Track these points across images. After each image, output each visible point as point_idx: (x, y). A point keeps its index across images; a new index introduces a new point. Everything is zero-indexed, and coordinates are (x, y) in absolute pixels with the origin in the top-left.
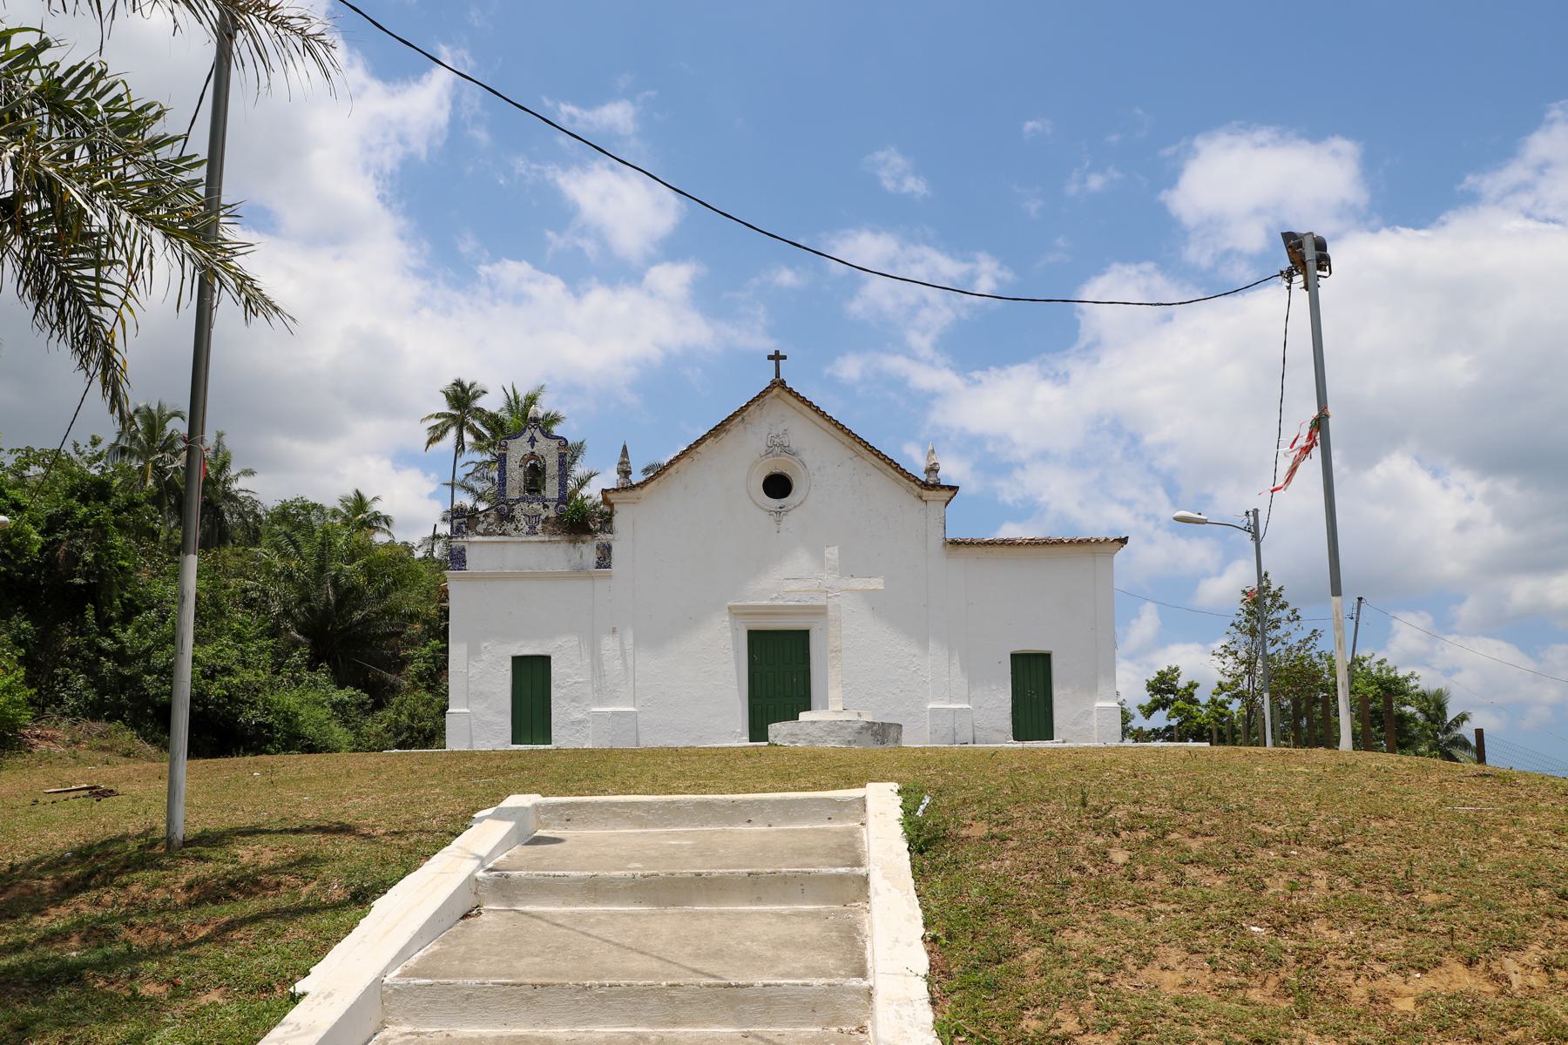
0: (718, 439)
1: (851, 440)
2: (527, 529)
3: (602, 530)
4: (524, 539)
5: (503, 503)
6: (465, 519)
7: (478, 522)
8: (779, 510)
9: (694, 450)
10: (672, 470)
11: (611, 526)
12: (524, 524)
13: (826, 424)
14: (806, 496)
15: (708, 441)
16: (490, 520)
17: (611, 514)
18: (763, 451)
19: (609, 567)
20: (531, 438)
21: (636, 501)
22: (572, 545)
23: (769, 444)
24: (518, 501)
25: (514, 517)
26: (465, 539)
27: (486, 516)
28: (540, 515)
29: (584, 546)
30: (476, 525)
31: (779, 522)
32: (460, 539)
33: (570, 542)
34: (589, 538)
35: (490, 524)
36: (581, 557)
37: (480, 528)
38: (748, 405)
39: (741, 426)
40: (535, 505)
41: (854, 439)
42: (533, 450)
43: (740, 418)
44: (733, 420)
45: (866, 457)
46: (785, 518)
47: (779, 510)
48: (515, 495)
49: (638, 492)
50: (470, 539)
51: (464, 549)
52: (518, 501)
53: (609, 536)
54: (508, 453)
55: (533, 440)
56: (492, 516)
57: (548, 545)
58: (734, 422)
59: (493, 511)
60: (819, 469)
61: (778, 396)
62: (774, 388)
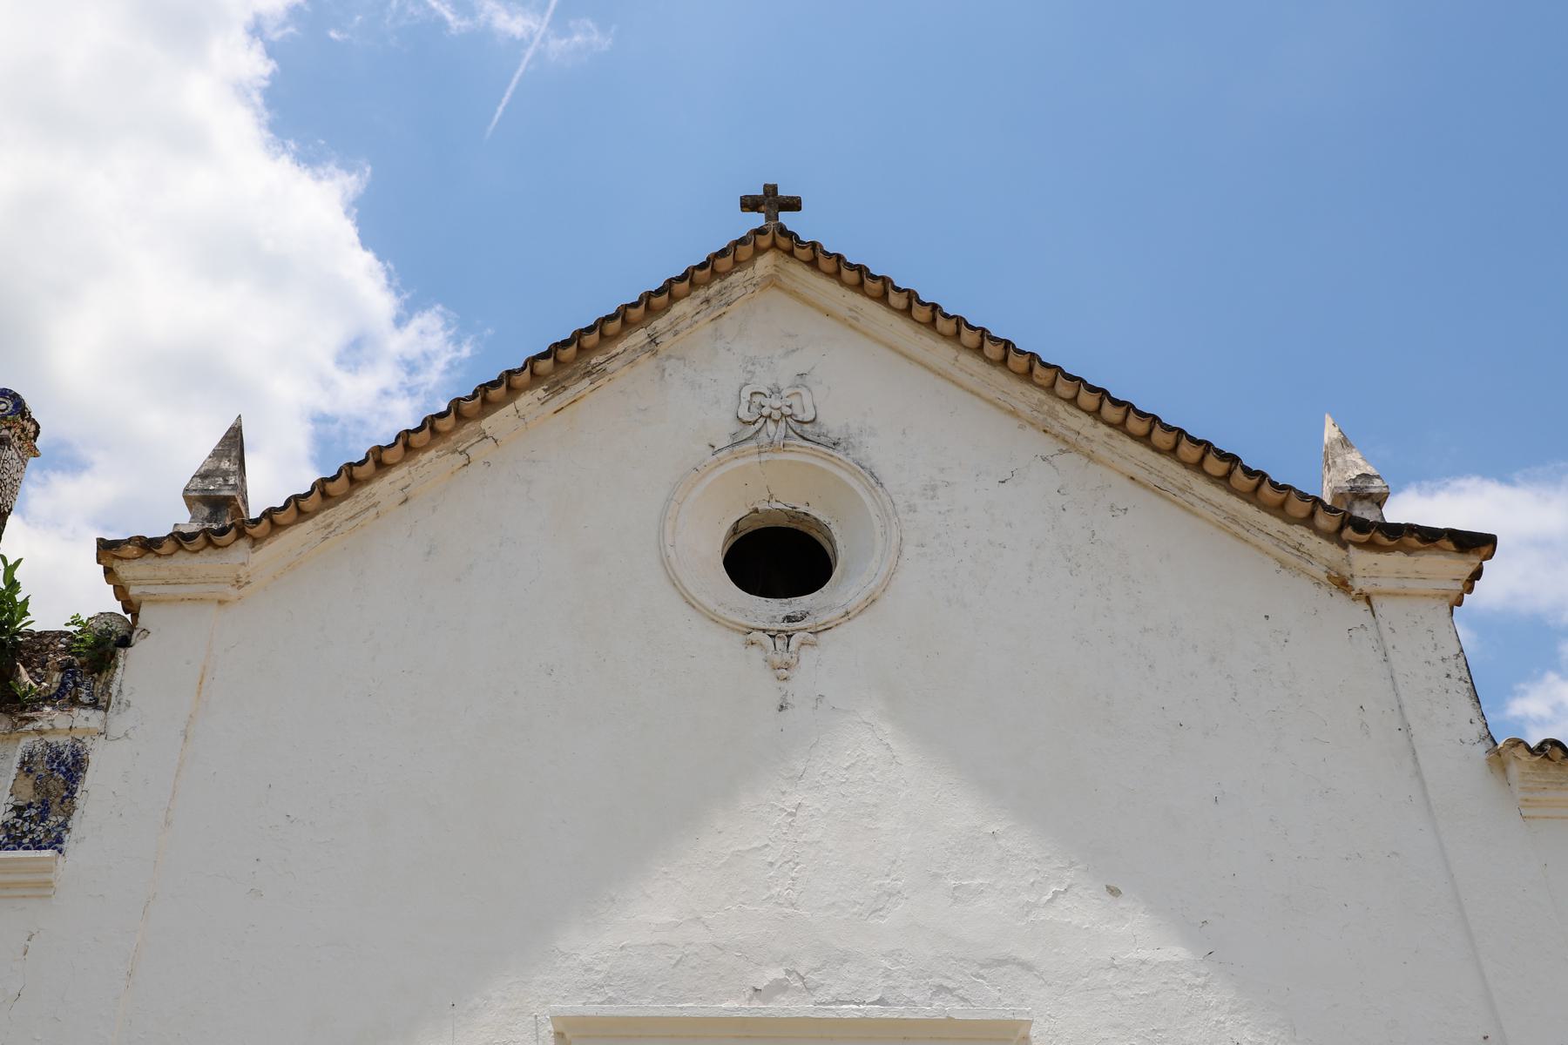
0: (555, 403)
1: (1040, 395)
3: (66, 697)
8: (785, 626)
9: (470, 427)
10: (384, 488)
11: (107, 685)
13: (942, 353)
14: (891, 575)
15: (525, 401)
17: (125, 642)
18: (722, 426)
19: (56, 843)
21: (233, 592)
23: (744, 414)
31: (782, 671)
38: (669, 291)
39: (646, 364)
41: (1050, 389)
43: (638, 337)
44: (617, 337)
45: (1102, 452)
46: (808, 656)
47: (785, 626)
53: (85, 719)
58: (620, 347)
60: (931, 490)
61: (772, 282)
62: (759, 251)
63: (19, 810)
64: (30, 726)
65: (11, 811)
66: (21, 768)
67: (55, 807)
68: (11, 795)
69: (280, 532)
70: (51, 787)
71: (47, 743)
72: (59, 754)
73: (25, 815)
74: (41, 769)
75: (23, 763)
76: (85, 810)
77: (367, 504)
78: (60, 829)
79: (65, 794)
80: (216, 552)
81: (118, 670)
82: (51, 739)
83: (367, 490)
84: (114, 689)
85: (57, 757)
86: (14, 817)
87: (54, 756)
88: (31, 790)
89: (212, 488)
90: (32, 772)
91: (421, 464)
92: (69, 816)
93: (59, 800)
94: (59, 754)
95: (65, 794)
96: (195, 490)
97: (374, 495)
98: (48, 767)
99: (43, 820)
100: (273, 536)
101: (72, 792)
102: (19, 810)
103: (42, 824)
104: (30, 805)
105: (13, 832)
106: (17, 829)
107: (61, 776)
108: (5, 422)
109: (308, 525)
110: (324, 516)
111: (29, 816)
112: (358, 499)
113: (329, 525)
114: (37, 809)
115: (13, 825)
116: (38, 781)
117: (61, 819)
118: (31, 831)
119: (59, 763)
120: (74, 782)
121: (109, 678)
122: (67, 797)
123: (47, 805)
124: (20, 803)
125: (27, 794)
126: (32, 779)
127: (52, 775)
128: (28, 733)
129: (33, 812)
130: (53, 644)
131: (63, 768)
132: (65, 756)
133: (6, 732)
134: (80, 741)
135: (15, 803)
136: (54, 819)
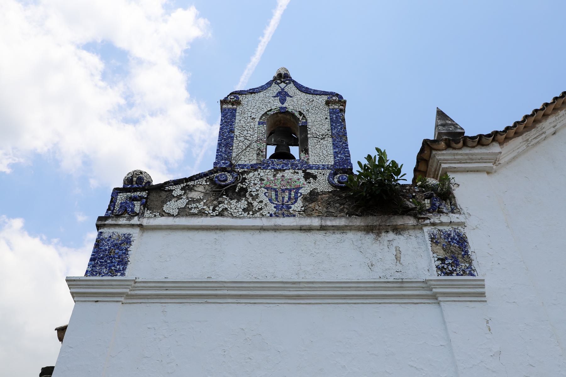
2: (271, 208)
4: (265, 222)
5: (224, 170)
6: (144, 194)
7: (170, 196)
12: (266, 200)
16: (194, 195)
20: (279, 93)
22: (372, 236)
24: (254, 168)
25: (245, 190)
26: (135, 221)
27: (187, 189)
28: (299, 188)
29: (400, 236)
30: (164, 202)
32: (122, 221)
33: (368, 229)
34: (411, 221)
35: (193, 201)
36: (398, 258)
37: (172, 206)
40: (288, 174)
42: (284, 106)
48: (250, 158)
49: (495, 148)
50: (145, 222)
51: (128, 240)
52: (254, 168)
53: (454, 217)
54: (239, 109)
55: (283, 96)
56: (201, 189)
57: (319, 236)
59: (203, 181)
63: (443, 260)
64: (428, 221)
65: (437, 260)
66: (431, 241)
67: (460, 259)
68: (434, 253)
69: (509, 140)
70: (453, 250)
71: (439, 230)
72: (449, 235)
73: (446, 263)
74: (443, 242)
75: (432, 238)
76: (478, 260)
77: (541, 132)
78: (469, 269)
79: (463, 253)
80: (483, 147)
81: (456, 199)
82: (441, 228)
83: (541, 124)
84: (459, 207)
85: (449, 235)
86: (441, 264)
87: (447, 236)
88: (443, 251)
89: (451, 129)
90: (439, 243)
91: (560, 116)
92: (470, 264)
93: (460, 256)
94: (449, 235)
95: (463, 253)
96: (444, 130)
97: (544, 128)
98: (446, 240)
99: (457, 265)
100: (507, 142)
101: (466, 252)
102: (443, 260)
103: (458, 267)
104: (446, 258)
105: (444, 271)
106: (445, 269)
107: (456, 245)
108: (340, 103)
109: (519, 139)
110: (526, 136)
111: (449, 263)
112: (538, 129)
113: (527, 140)
114: (451, 259)
115: (443, 267)
116: (444, 247)
117: (468, 265)
118: (455, 270)
119: (451, 239)
120: (465, 248)
121: (453, 202)
122: (465, 255)
123: (455, 258)
124: (440, 257)
125: (442, 254)
126: (440, 246)
127: (451, 245)
128: (426, 225)
129: (451, 261)
130: (411, 189)
131: (455, 241)
132: (452, 235)
133: (415, 224)
134: (458, 229)
135: (438, 257)
136: (463, 265)
